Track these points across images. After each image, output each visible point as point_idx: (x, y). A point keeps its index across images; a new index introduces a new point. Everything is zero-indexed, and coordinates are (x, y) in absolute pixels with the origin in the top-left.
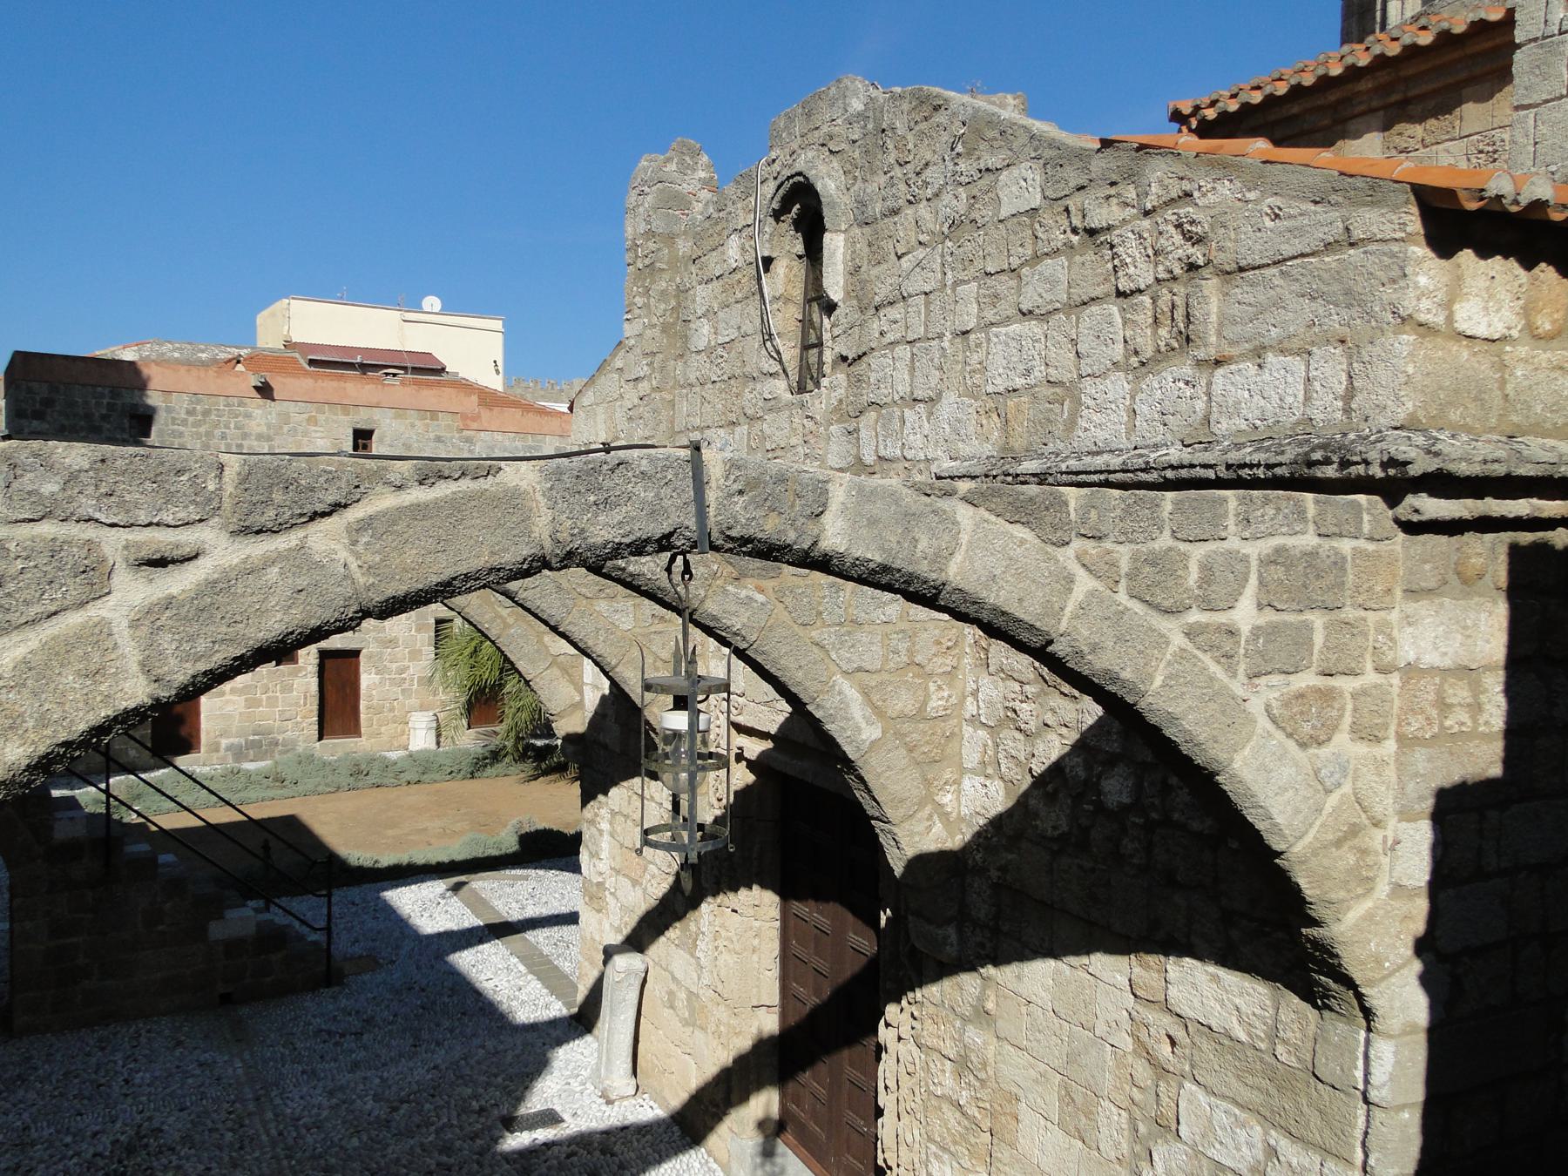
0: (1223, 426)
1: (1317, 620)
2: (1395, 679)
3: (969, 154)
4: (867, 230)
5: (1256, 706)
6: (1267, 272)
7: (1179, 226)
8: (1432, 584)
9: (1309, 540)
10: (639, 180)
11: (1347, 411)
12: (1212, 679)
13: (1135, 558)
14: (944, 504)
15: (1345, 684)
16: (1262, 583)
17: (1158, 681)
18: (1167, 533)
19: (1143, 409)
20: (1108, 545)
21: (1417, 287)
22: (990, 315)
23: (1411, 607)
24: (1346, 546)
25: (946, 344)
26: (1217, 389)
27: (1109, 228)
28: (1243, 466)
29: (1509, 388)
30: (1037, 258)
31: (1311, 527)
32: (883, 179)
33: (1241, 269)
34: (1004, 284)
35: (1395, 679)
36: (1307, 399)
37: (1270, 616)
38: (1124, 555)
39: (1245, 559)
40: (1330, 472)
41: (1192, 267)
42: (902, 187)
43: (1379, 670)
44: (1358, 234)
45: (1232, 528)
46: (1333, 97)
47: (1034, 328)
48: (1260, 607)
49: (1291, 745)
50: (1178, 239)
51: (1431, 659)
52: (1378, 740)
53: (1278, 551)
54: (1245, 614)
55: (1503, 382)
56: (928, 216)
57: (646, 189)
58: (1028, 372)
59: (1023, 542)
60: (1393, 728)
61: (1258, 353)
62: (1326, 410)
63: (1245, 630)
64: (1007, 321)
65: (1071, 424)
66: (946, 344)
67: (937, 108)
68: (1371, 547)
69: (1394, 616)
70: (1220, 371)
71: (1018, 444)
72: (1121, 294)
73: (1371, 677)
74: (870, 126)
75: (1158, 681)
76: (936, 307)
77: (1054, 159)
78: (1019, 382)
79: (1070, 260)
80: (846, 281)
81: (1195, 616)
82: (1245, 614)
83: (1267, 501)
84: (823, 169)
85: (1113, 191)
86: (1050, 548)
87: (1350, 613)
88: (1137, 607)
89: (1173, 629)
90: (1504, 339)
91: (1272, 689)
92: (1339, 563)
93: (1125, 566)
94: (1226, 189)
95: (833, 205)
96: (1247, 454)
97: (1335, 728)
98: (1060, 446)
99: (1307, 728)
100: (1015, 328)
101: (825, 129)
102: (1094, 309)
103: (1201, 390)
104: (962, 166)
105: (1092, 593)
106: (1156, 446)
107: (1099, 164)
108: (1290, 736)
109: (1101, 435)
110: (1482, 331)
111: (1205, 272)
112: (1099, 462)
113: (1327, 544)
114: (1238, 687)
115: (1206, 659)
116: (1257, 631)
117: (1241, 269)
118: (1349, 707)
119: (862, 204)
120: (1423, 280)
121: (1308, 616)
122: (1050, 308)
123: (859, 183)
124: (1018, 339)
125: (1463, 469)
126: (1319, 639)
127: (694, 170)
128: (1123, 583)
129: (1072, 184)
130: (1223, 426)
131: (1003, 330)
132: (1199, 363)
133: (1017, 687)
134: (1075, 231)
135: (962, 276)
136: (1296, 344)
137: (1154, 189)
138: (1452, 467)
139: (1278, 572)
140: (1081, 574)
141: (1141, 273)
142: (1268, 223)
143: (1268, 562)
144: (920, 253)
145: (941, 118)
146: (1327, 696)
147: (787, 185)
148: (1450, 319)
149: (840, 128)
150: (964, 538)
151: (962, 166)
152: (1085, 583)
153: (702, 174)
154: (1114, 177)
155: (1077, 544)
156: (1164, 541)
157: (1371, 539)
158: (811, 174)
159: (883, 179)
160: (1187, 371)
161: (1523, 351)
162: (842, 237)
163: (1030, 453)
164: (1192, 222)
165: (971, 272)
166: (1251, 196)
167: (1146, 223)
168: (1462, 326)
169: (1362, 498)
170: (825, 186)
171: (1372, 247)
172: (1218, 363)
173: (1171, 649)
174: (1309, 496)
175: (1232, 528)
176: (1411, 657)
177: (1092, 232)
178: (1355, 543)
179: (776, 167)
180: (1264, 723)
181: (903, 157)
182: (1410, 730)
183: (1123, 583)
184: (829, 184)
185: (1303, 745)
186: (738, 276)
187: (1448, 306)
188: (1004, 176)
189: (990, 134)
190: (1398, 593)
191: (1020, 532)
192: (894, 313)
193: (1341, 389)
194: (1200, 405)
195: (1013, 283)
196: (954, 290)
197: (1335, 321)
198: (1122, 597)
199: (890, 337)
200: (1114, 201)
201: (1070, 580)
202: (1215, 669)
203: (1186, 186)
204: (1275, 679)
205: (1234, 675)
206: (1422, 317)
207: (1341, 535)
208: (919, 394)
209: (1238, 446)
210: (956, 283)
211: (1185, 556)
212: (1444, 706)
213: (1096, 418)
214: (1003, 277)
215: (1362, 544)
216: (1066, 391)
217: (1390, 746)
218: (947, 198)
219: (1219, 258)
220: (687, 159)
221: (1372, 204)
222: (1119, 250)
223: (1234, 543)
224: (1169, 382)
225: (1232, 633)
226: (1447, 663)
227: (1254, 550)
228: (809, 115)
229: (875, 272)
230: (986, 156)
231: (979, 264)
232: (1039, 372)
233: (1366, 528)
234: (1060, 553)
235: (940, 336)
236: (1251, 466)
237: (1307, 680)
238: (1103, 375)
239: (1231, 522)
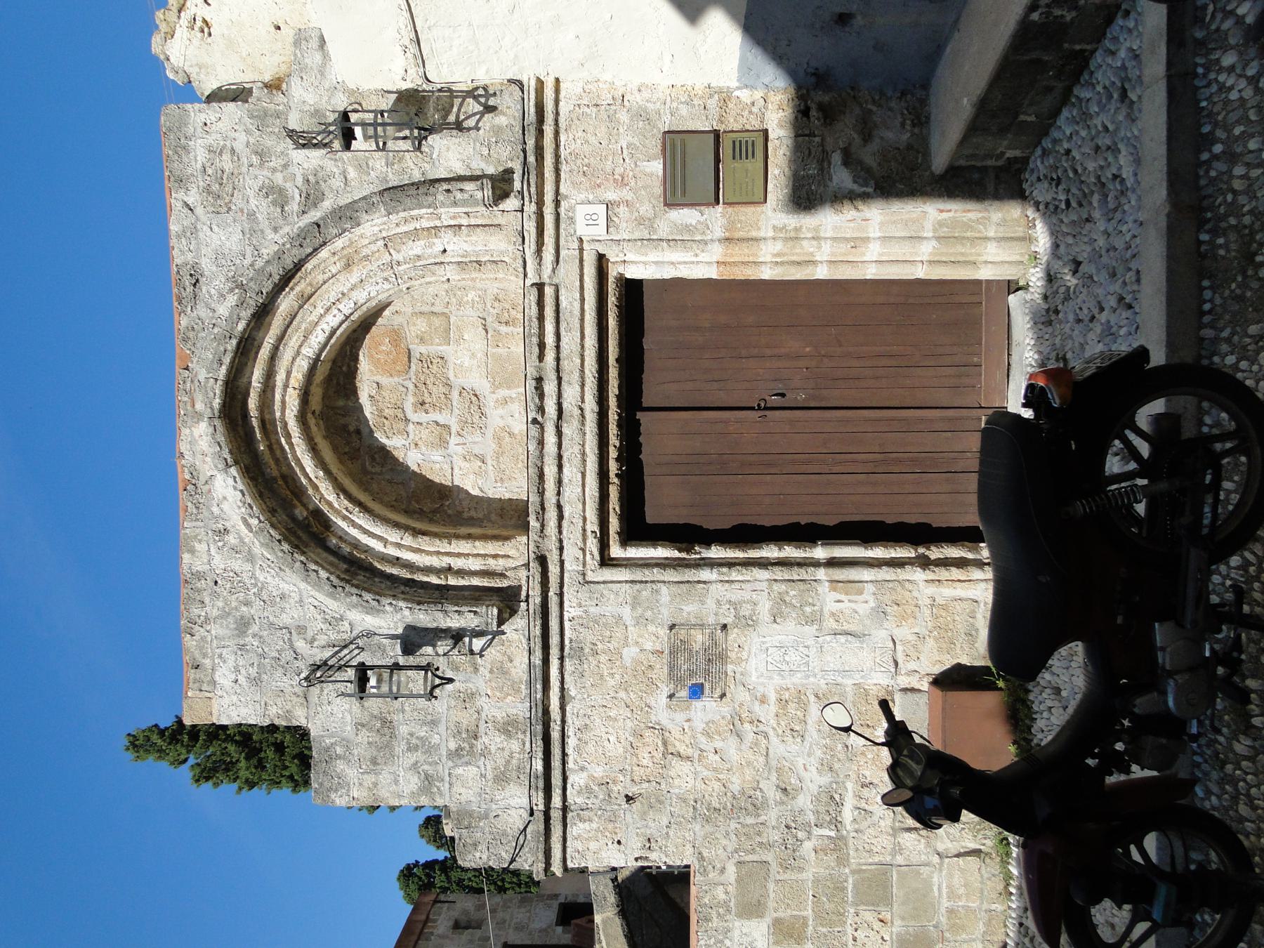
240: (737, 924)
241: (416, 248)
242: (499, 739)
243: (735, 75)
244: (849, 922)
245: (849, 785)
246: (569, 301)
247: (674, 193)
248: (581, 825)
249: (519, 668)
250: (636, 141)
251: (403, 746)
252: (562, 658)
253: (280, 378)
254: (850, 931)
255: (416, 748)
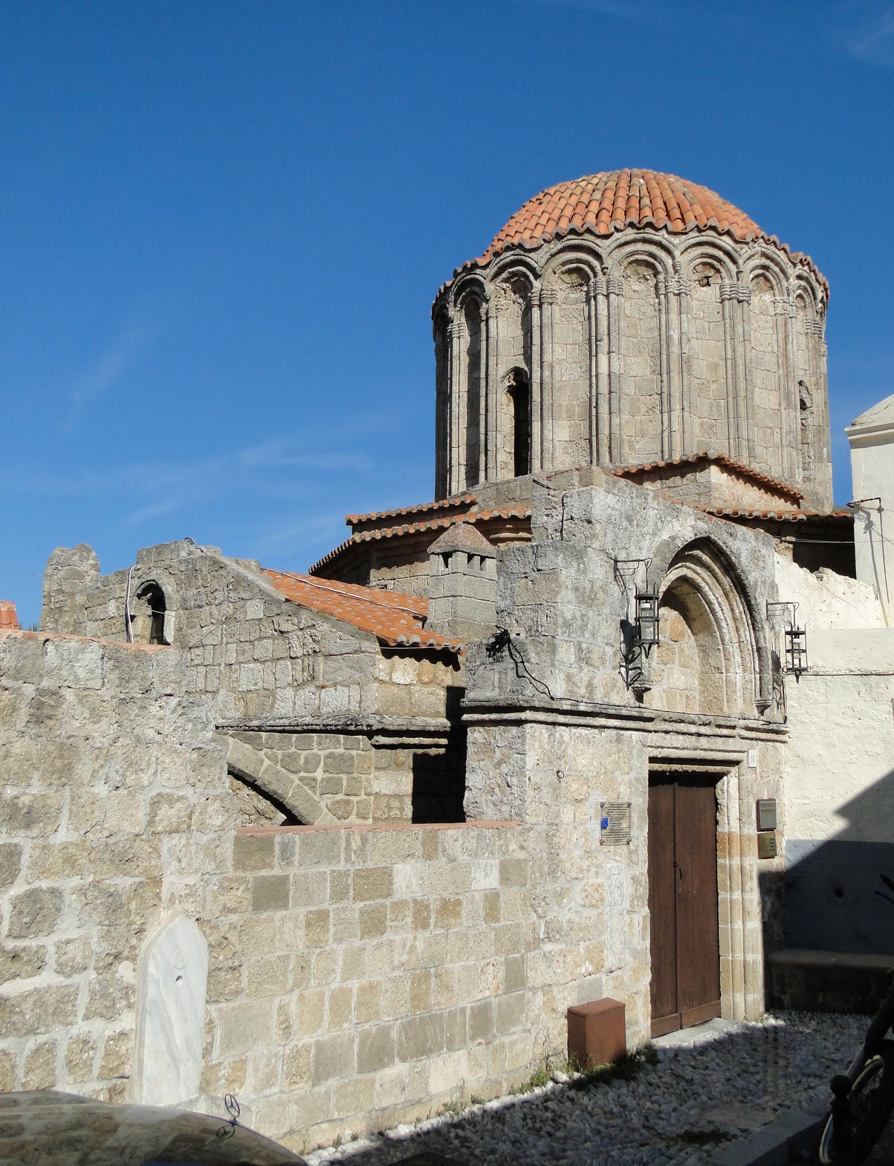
0: (324, 710)
1: (344, 777)
2: (372, 798)
3: (235, 590)
4: (186, 612)
5: (323, 804)
6: (338, 657)
7: (311, 636)
8: (385, 766)
9: (341, 750)
10: (55, 561)
11: (360, 707)
12: (308, 794)
13: (283, 755)
14: (224, 737)
15: (355, 799)
16: (325, 764)
17: (290, 794)
18: (294, 747)
19: (298, 702)
20: (275, 750)
21: (379, 668)
22: (241, 659)
23: (377, 773)
24: (354, 753)
25: (222, 668)
26: (322, 696)
27: (288, 632)
28: (328, 725)
29: (413, 701)
30: (261, 638)
31: (342, 746)
32: (195, 591)
33: (330, 655)
34: (247, 647)
35: (372, 798)
36: (349, 702)
37: (328, 775)
38: (280, 754)
39: (319, 756)
40: (352, 728)
41: (315, 652)
42: (204, 596)
43: (366, 794)
44: (363, 649)
45: (315, 746)
46: (412, 541)
47: (258, 666)
48: (324, 772)
49: (335, 818)
50: (311, 640)
51: (384, 791)
52: (366, 819)
53: (330, 753)
54: (319, 774)
55: (411, 698)
56: (216, 612)
57: (60, 567)
58: (256, 684)
59: (248, 749)
60: (371, 815)
61: (335, 685)
62: (354, 707)
63: (319, 779)
64: (248, 662)
65: (272, 706)
66: (222, 668)
67: (222, 568)
68: (363, 753)
69: (372, 776)
70: (323, 690)
71: (251, 713)
72: (291, 658)
73: (363, 797)
74: (190, 566)
75: (290, 794)
76: (218, 652)
77: (269, 600)
78: (252, 688)
79: (273, 641)
80: (175, 633)
81: (302, 774)
82: (319, 774)
83: (327, 737)
84: (165, 580)
85: (289, 618)
86: (256, 751)
87: (355, 775)
88: (283, 770)
89: (295, 778)
90: (410, 684)
91: (328, 799)
92: (352, 758)
93: (280, 757)
94: (326, 626)
95: (170, 598)
96: (330, 721)
97: (350, 813)
98: (268, 715)
99: (340, 813)
100: (251, 665)
101: (167, 562)
102: (282, 662)
103: (317, 697)
104: (231, 595)
105: (269, 765)
106: (302, 717)
107: (285, 607)
108: (334, 815)
109: (283, 711)
110: (402, 682)
111: (319, 654)
112: (281, 722)
113: (347, 752)
114: (316, 798)
115: (306, 788)
116: (323, 780)
117: (330, 655)
118: (356, 806)
119: (185, 600)
120: (381, 666)
121: (341, 775)
122: (265, 659)
123: (183, 590)
124: (253, 670)
125: (391, 728)
126: (345, 783)
127: (87, 560)
128: (279, 762)
129: (275, 612)
130: (324, 710)
131: (247, 665)
132: (317, 687)
133: (247, 817)
134: (275, 630)
135: (230, 640)
136: (346, 683)
137: (303, 621)
138: (387, 727)
139: (331, 761)
140: (266, 759)
141: (298, 651)
142: (338, 641)
143: (327, 757)
144: (212, 627)
145: (222, 572)
146: (347, 802)
147: (146, 584)
148: (391, 678)
149: (174, 563)
150: (230, 748)
151: (231, 595)
152: (267, 762)
153: (92, 562)
154: (290, 614)
155: (265, 750)
156: (293, 749)
157: (363, 750)
158: (160, 582)
159: (195, 591)
160: (313, 689)
161: (418, 688)
162: (174, 613)
163: (256, 717)
164: (315, 636)
165: (234, 639)
166: (333, 630)
167: (300, 633)
168: (395, 680)
169: (360, 737)
170: (166, 589)
171: (367, 654)
172: (323, 687)
173: (295, 784)
174: (342, 736)
175: (315, 746)
176: (377, 790)
177: (282, 632)
178: (357, 752)
179: (140, 572)
180: (325, 810)
181: (205, 584)
182: (377, 816)
183: (279, 762)
184: (169, 588)
185: (339, 819)
186: (114, 621)
187: (390, 674)
188: (249, 603)
189: (244, 584)
190: (373, 769)
191: (247, 746)
192: (199, 651)
193: (358, 700)
194: (317, 702)
195: (251, 647)
196: (226, 646)
197: (357, 676)
198: (279, 767)
199: (196, 662)
200: (290, 622)
201: (262, 761)
202: (308, 791)
203: (314, 623)
204: (329, 796)
205: (316, 794)
206: (381, 678)
207: (352, 749)
208: (209, 689)
209: (328, 718)
210: (227, 643)
211: (300, 755)
212: (390, 809)
213: (282, 704)
214: (247, 644)
215: (360, 752)
216: (270, 693)
217: (370, 821)
218: (224, 606)
219: (323, 650)
220: (84, 553)
221: (367, 640)
222: (292, 641)
223: (315, 751)
224: (307, 692)
225: (315, 780)
226: (391, 793)
227: (323, 753)
228: (159, 553)
229: (189, 631)
230: (242, 593)
231: (237, 636)
232: (260, 684)
233: (361, 747)
234: (260, 753)
235: (220, 665)
236: (330, 725)
237: (341, 797)
238: (284, 688)
239: (315, 744)
240: (497, 862)
241: (738, 658)
242: (586, 679)
243: (792, 838)
244: (498, 958)
245: (563, 946)
246: (731, 744)
247: (764, 805)
248: (546, 736)
249: (616, 699)
250: (771, 784)
251: (584, 612)
252: (616, 728)
253: (698, 569)
254: (492, 959)
255: (582, 620)
